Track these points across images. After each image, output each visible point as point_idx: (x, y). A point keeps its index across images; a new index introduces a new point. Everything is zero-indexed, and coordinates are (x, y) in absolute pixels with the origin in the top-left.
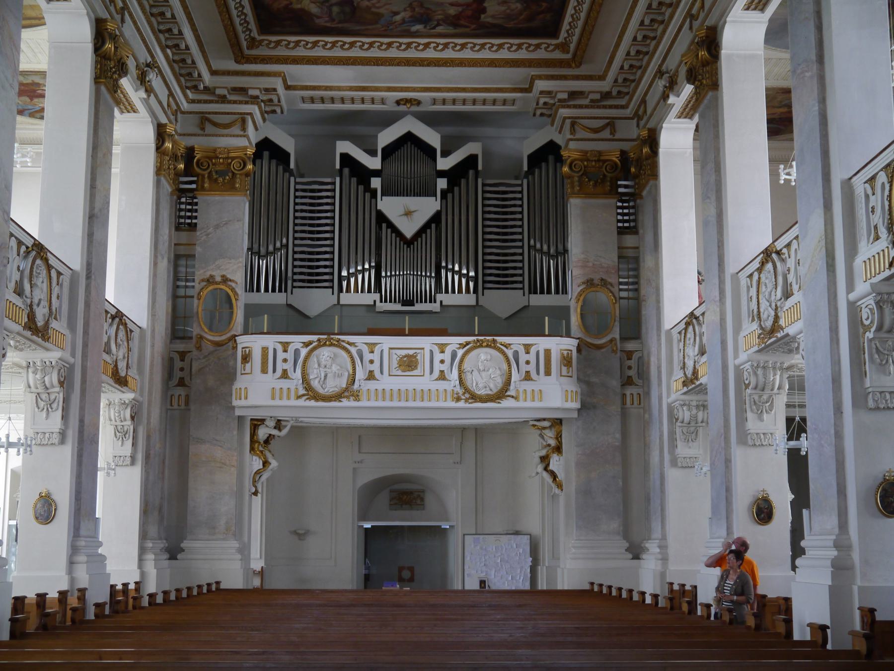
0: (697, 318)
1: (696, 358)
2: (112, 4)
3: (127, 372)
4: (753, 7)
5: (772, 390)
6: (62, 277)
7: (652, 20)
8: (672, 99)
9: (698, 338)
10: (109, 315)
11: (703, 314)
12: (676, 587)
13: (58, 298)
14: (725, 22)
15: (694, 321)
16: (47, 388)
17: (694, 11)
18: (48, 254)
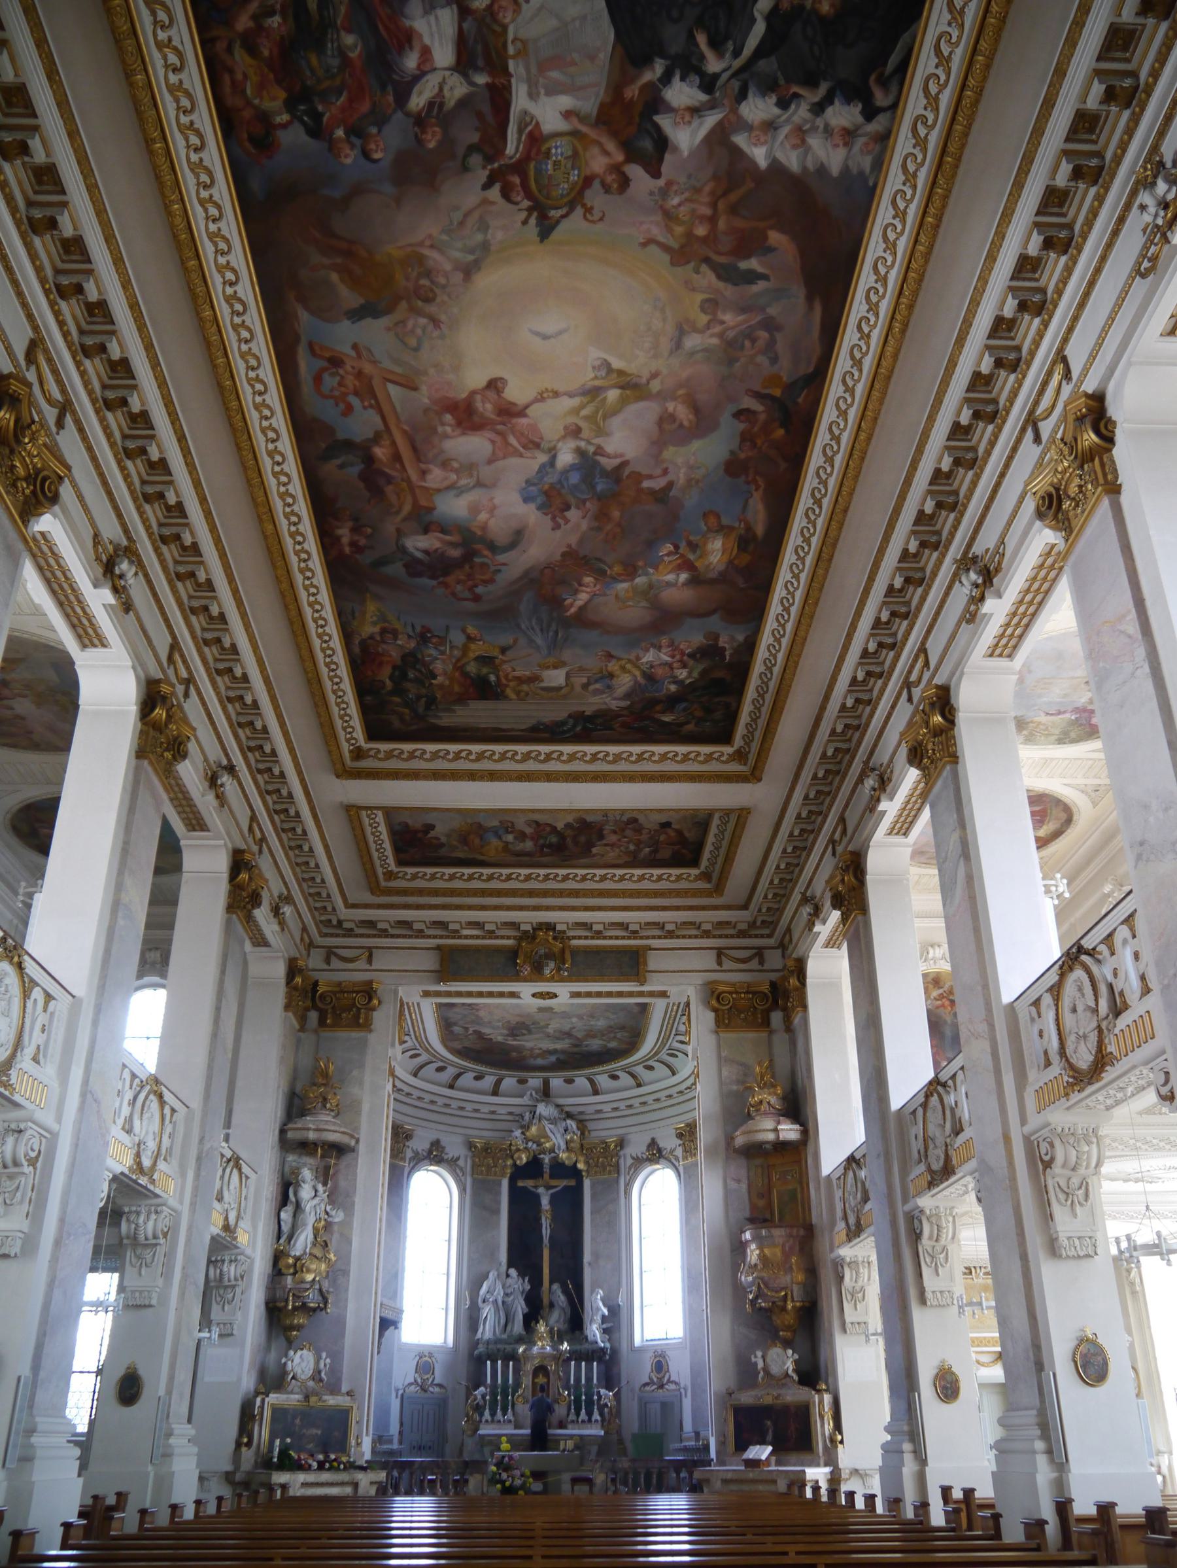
0: (944, 1085)
1: (948, 1140)
2: (172, 667)
3: (155, 1164)
4: (998, 652)
5: (1087, 1168)
6: (52, 1003)
7: (847, 726)
8: (883, 806)
9: (948, 1113)
10: (137, 1081)
11: (954, 1077)
12: (957, 1494)
13: (43, 1031)
14: (962, 674)
15: (939, 1088)
16: (5, 1167)
17: (913, 678)
18: (26, 957)
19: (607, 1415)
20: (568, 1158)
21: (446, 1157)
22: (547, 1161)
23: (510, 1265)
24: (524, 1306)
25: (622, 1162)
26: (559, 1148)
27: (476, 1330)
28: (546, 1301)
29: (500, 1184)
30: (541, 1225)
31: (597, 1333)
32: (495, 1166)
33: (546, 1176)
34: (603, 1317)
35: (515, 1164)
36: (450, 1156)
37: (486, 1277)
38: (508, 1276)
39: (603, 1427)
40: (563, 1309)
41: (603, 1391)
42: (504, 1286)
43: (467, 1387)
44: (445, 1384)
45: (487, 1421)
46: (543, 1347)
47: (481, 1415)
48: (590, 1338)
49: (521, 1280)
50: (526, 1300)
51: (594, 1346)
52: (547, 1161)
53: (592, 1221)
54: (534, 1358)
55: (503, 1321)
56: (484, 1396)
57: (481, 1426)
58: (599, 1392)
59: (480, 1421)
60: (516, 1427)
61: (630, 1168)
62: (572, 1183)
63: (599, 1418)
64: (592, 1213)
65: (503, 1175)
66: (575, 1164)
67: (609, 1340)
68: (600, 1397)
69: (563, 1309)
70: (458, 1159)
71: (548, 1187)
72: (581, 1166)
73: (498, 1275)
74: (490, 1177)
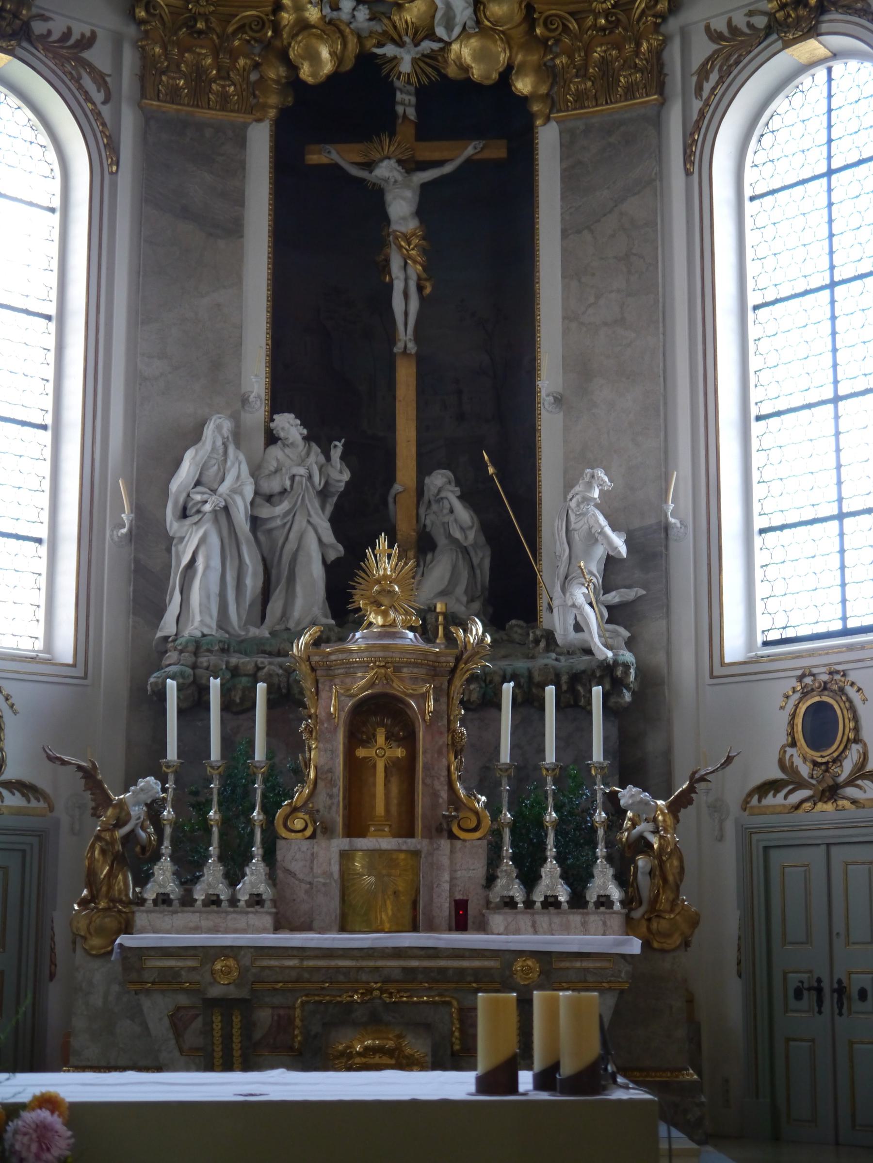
19: (643, 881)
20: (480, 55)
21: (38, 28)
22: (406, 67)
23: (276, 405)
24: (329, 537)
25: (674, 54)
26: (449, 28)
27: (160, 612)
28: (405, 527)
29: (241, 142)
30: (390, 287)
31: (591, 614)
32: (224, 75)
33: (406, 132)
34: (611, 562)
35: (295, 83)
36: (57, 27)
37: (195, 436)
38: (271, 438)
39: (630, 926)
40: (465, 551)
41: (628, 795)
42: (255, 473)
43: (89, 775)
44: (42, 784)
45: (163, 900)
46: (389, 630)
47: (143, 879)
48: (564, 632)
49: (315, 448)
50: (334, 521)
51: (582, 663)
52: (406, 67)
53: (567, 255)
54: (350, 669)
55: (252, 582)
56: (154, 809)
57: (141, 918)
58: (613, 798)
59: (140, 901)
60: (277, 927)
61: (703, 73)
62: (498, 151)
63: (615, 893)
64: (565, 234)
65: (255, 110)
66: (509, 68)
67: (630, 644)
68: (616, 811)
69: (465, 551)
70: (87, 42)
71: (411, 166)
72: (523, 85)
73: (238, 437)
74: (205, 115)
